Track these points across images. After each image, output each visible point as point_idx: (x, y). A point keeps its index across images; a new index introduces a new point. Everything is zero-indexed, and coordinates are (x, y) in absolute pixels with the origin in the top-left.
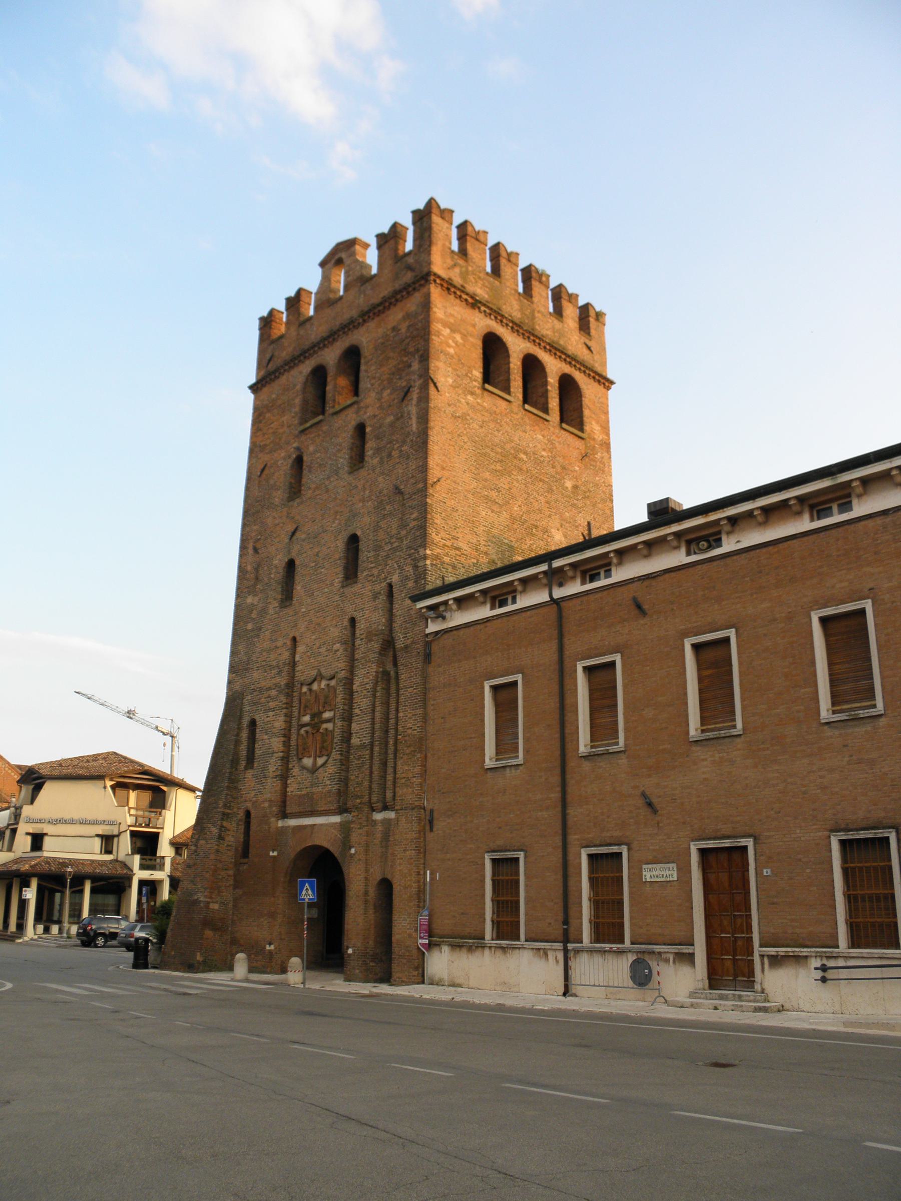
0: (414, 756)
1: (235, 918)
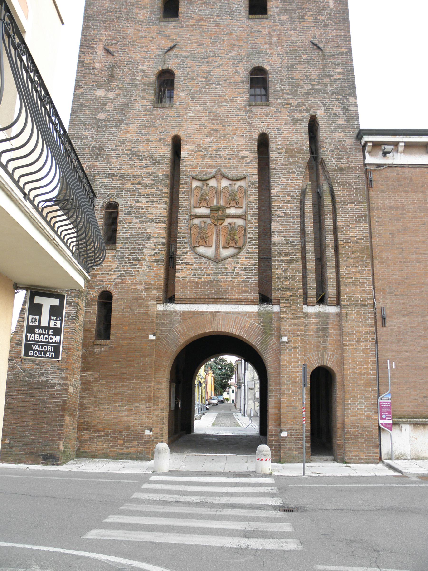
0: (362, 261)
1: (86, 402)
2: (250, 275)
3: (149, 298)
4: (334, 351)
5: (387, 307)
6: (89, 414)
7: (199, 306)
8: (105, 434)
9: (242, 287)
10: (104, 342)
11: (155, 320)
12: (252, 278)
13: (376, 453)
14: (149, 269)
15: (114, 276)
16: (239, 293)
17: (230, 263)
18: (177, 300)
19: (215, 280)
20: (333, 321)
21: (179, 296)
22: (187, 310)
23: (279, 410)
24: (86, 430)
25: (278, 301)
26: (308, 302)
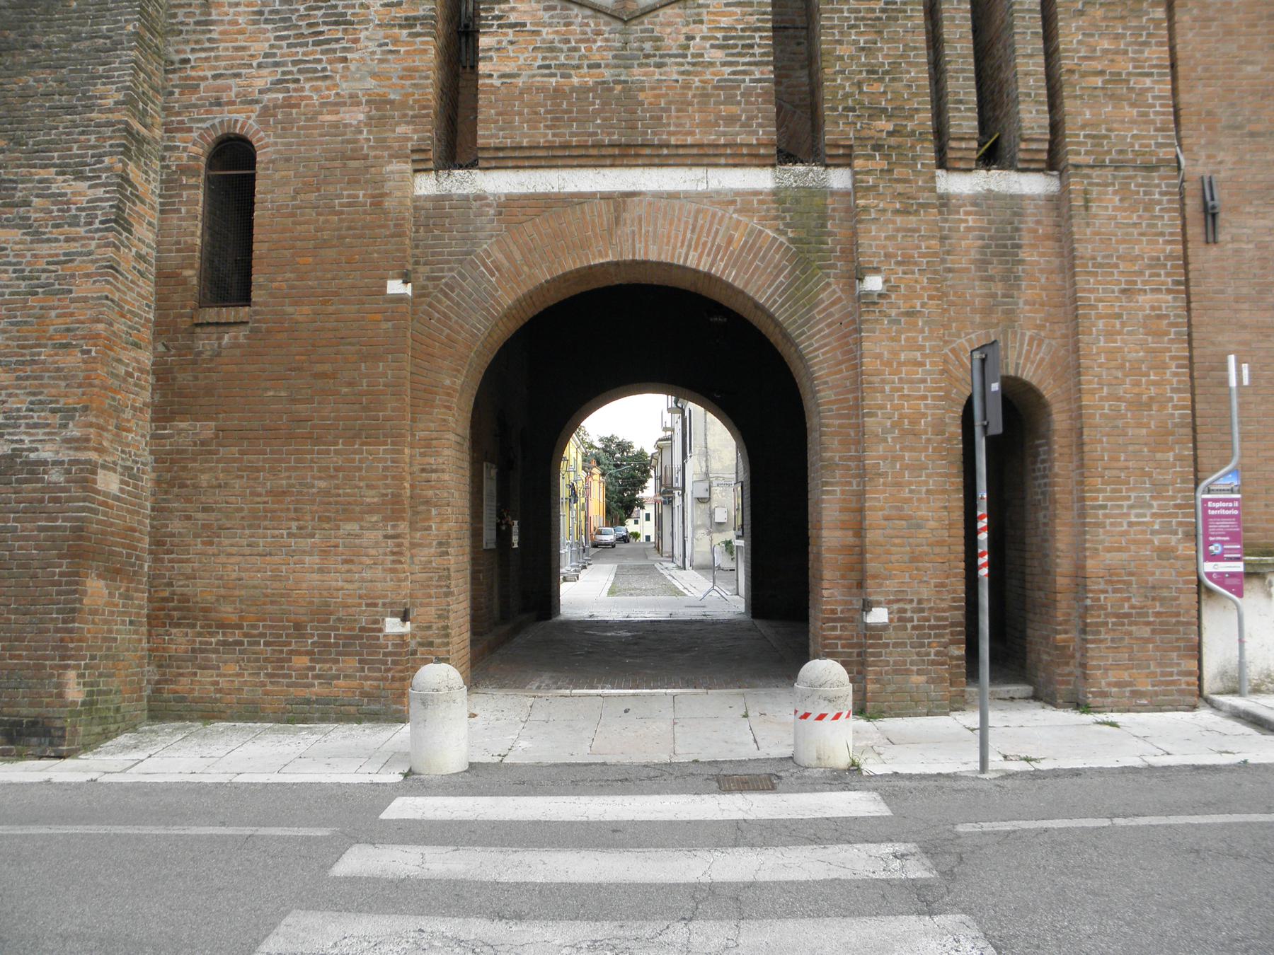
1: (176, 526)
2: (744, 64)
3: (386, 154)
4: (1042, 327)
5: (1223, 175)
6: (188, 568)
7: (565, 173)
8: (246, 635)
9: (717, 103)
10: (228, 314)
11: (409, 227)
12: (752, 73)
13: (1190, 674)
14: (384, 52)
15: (260, 83)
16: (705, 124)
17: (670, 24)
18: (486, 155)
19: (619, 82)
20: (1038, 222)
21: (493, 142)
22: (523, 190)
23: (859, 531)
24: (178, 625)
25: (847, 152)
26: (951, 154)
